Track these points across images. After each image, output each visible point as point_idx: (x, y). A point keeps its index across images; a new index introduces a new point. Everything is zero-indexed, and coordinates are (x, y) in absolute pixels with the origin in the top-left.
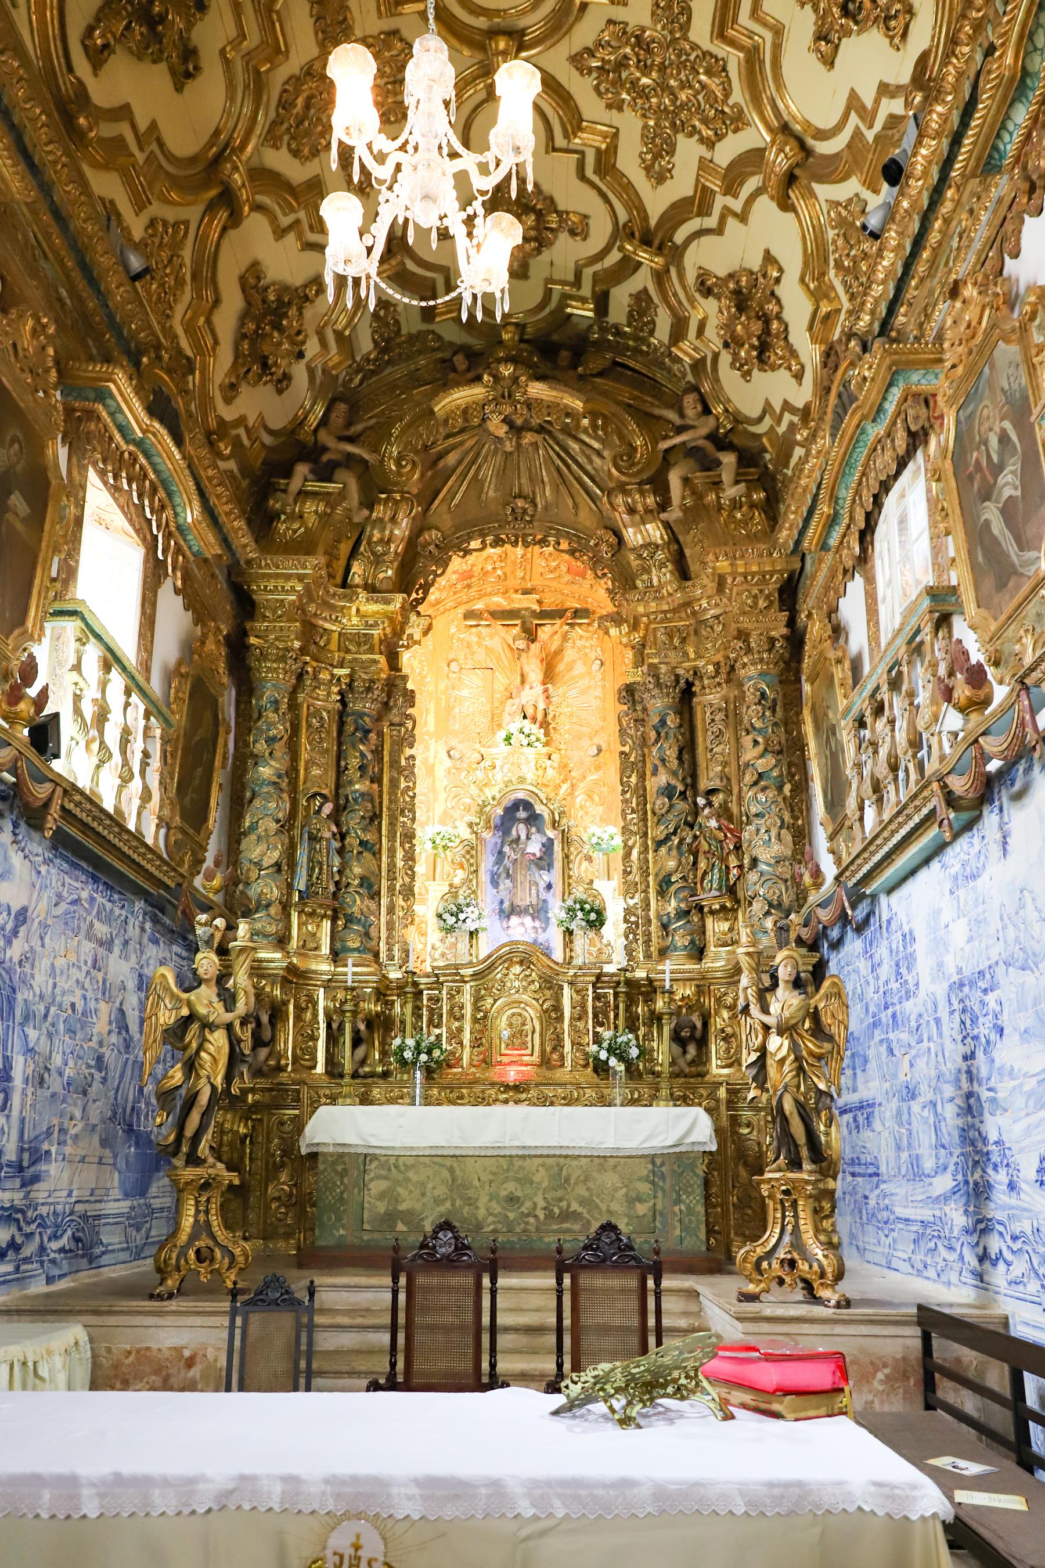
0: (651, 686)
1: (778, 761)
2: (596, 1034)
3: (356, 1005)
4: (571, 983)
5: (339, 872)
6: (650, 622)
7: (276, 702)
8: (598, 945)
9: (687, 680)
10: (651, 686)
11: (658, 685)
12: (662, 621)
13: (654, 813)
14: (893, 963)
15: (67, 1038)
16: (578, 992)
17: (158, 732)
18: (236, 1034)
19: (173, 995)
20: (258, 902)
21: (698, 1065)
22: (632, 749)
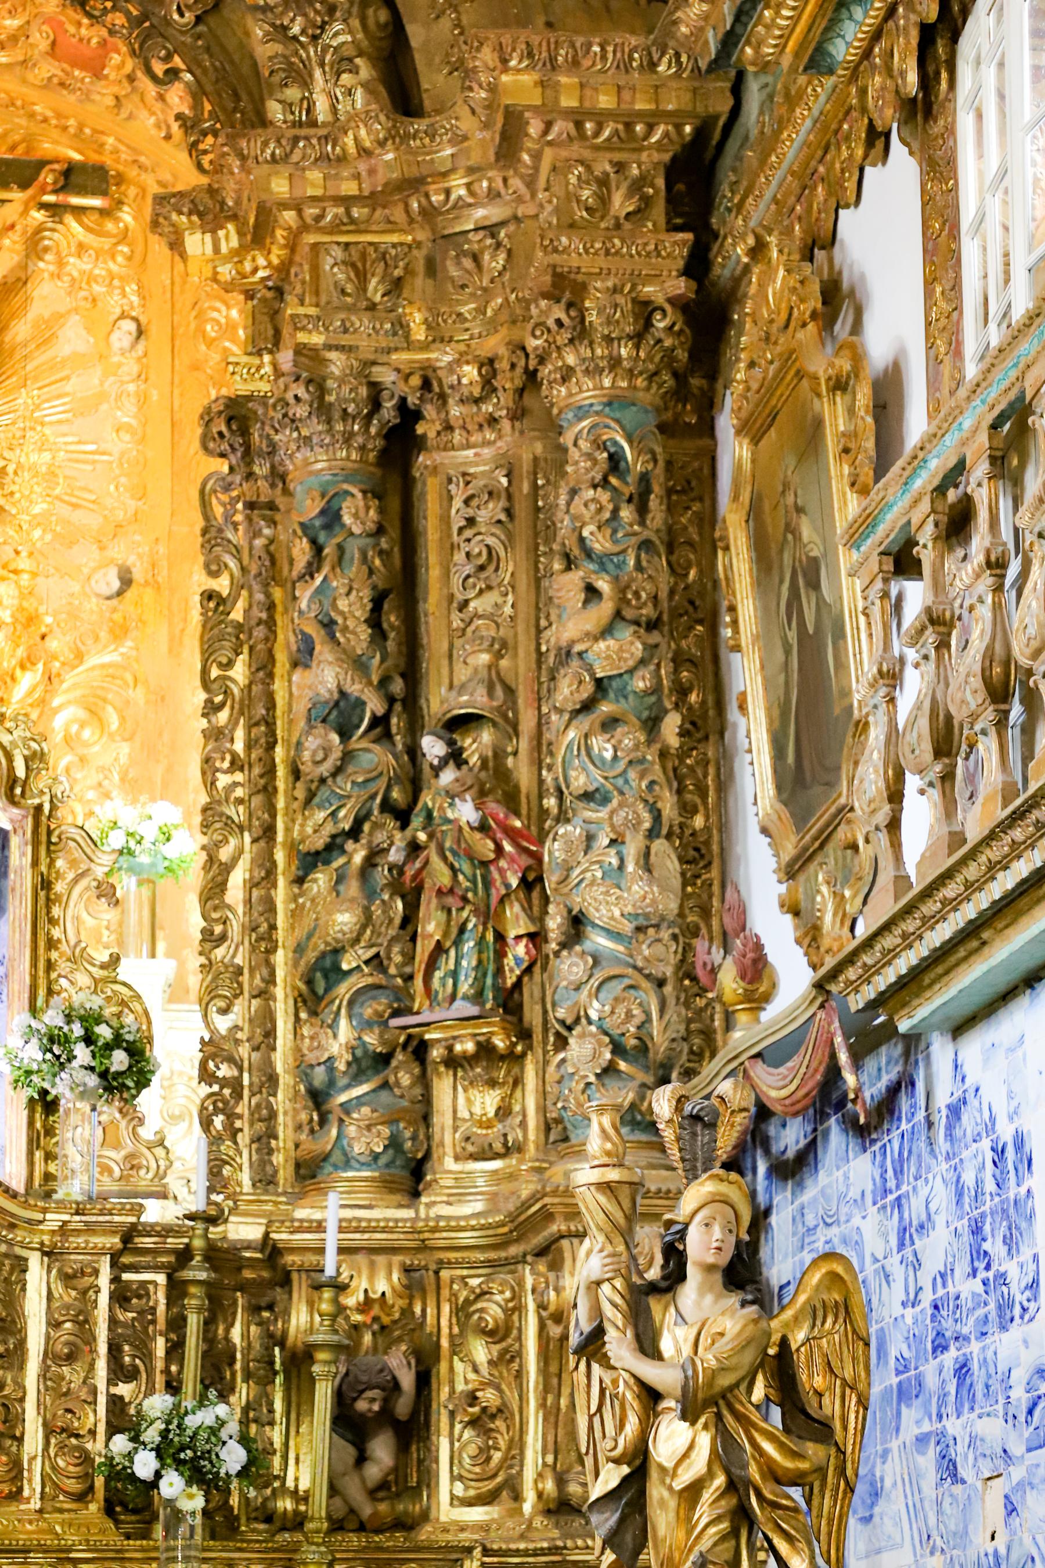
0: (301, 411)
1: (651, 649)
2: (116, 1404)
4: (49, 1253)
6: (304, 228)
8: (129, 1146)
9: (403, 400)
10: (301, 411)
11: (322, 409)
12: (336, 228)
13: (296, 774)
14: (963, 1225)
16: (68, 1279)
21: (398, 1495)
22: (237, 587)
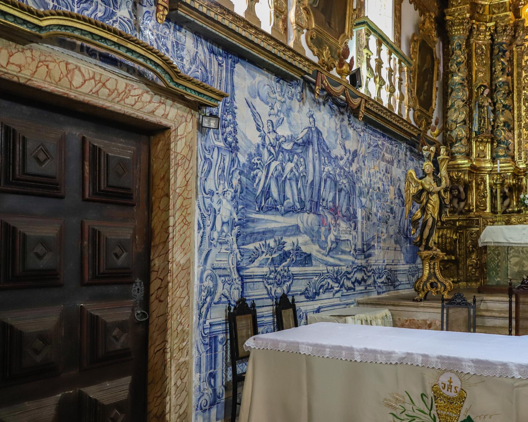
3: (503, 181)
5: (494, 121)
7: (460, 45)
17: (406, 68)
18: (442, 196)
19: (415, 181)
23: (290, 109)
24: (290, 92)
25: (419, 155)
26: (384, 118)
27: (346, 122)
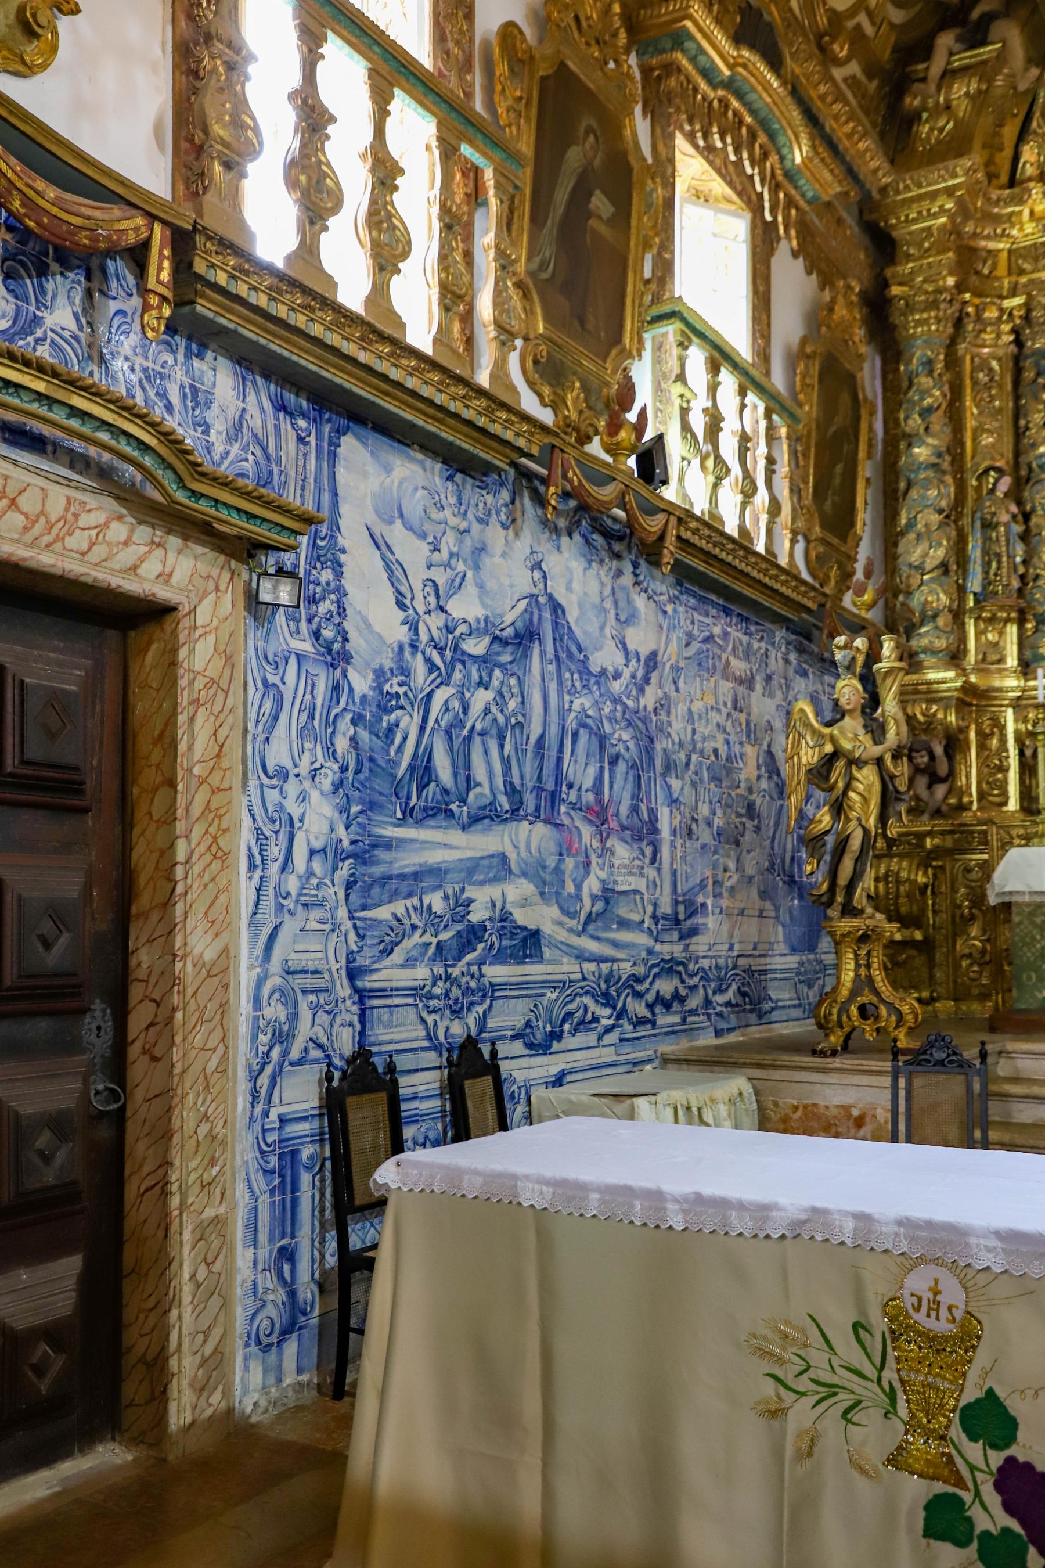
5: (1025, 562)
7: (930, 363)
15: (712, 786)
17: (783, 431)
18: (887, 770)
19: (814, 732)
20: (923, 613)
23: (481, 549)
24: (481, 505)
25: (823, 660)
26: (729, 564)
27: (627, 579)
